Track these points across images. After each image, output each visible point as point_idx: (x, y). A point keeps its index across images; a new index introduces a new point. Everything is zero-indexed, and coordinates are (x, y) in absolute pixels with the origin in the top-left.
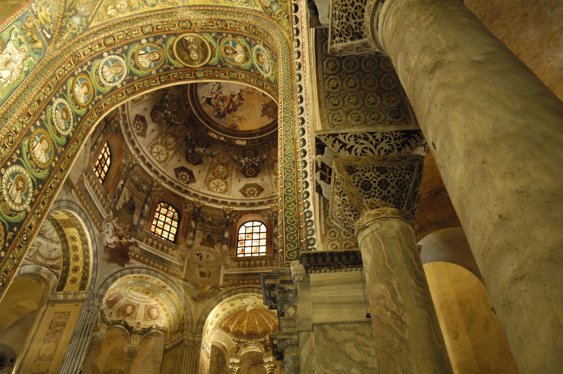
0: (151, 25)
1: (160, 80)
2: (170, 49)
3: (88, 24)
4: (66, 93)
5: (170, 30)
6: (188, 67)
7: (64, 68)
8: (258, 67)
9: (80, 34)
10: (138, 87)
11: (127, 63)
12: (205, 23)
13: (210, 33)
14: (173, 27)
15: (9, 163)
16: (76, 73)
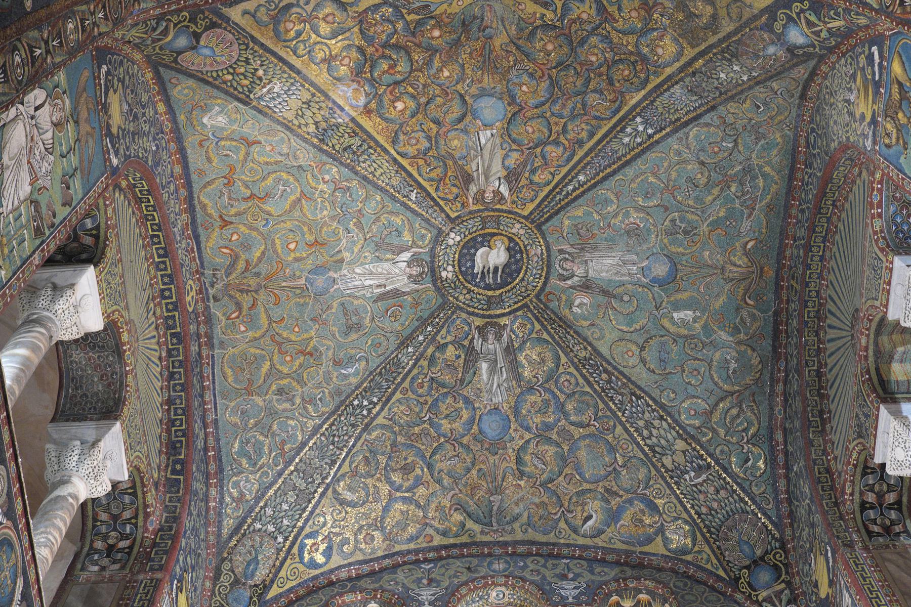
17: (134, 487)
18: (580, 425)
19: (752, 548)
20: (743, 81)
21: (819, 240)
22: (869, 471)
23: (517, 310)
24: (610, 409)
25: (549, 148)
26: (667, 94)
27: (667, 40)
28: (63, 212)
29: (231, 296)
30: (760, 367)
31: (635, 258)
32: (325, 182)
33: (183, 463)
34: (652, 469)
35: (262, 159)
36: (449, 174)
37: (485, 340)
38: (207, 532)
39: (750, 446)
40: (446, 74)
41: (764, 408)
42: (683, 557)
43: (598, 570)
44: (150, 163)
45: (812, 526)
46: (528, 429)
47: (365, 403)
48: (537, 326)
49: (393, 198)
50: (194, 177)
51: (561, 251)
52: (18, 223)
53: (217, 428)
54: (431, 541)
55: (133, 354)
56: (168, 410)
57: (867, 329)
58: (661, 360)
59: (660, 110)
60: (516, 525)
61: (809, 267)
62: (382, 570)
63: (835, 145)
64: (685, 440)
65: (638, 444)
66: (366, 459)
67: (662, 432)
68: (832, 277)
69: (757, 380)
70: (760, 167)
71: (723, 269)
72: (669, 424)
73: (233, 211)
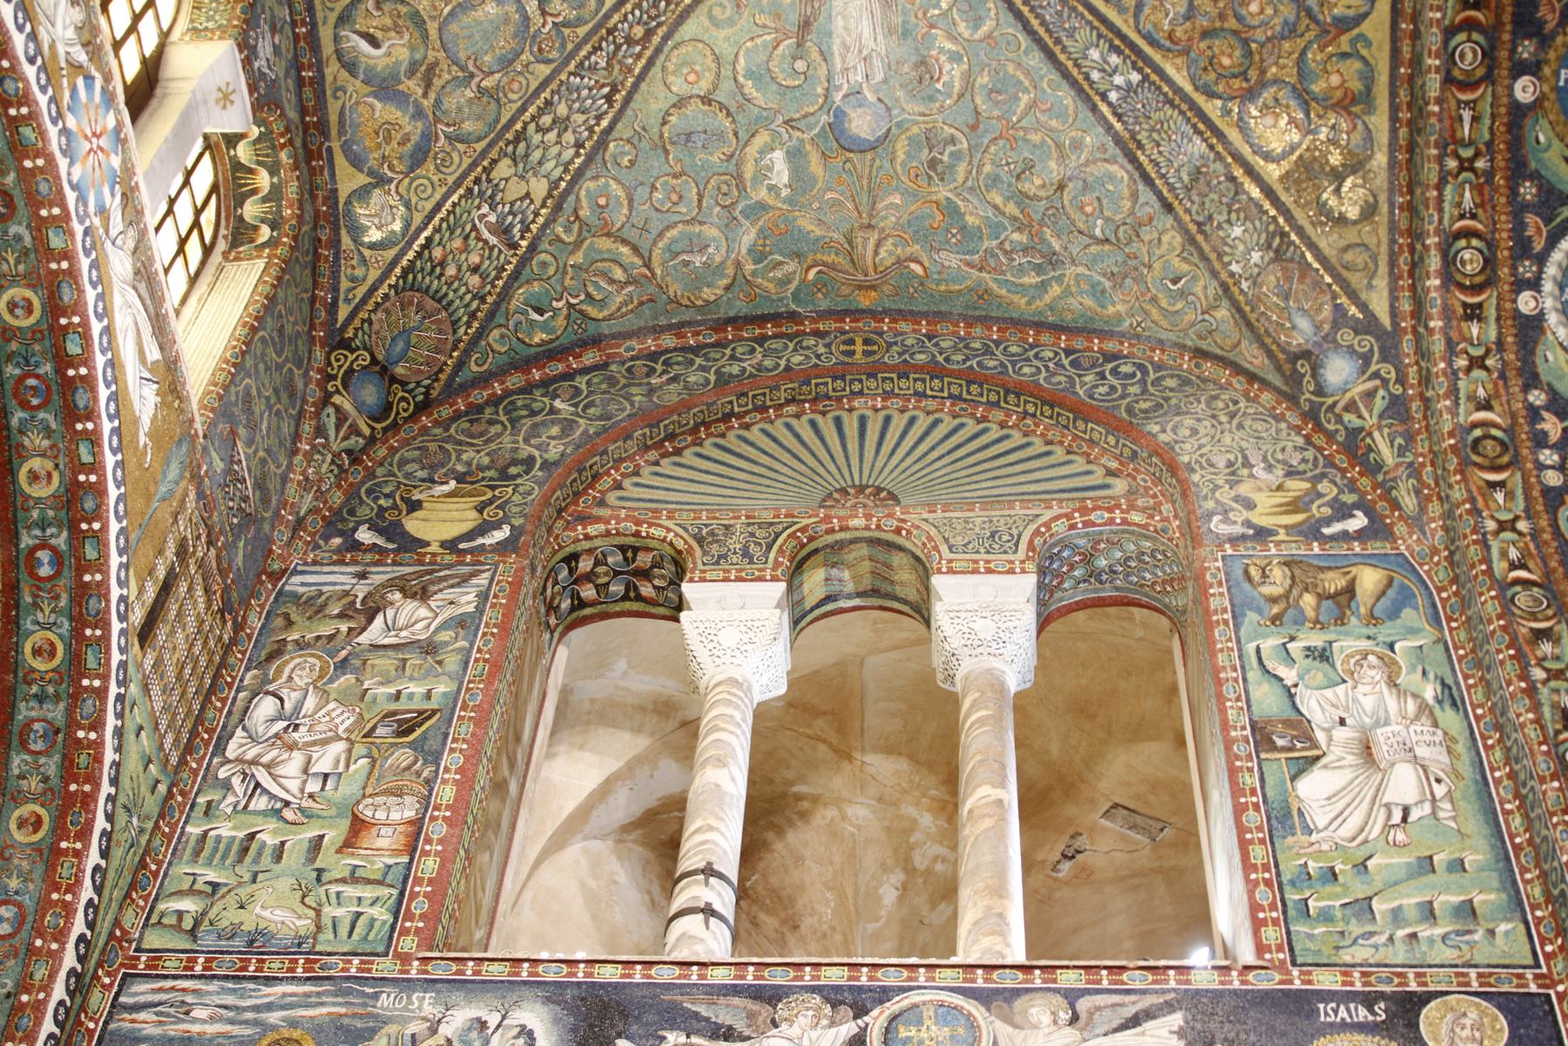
0: (1449, 32)
3: (1369, 325)
7: (1503, 526)
9: (1401, 380)
19: (403, 356)
20: (1230, 263)
21: (955, 390)
22: (630, 554)
24: (578, 47)
26: (1189, 130)
27: (1295, 136)
30: (699, 303)
31: (879, 77)
34: (483, 144)
39: (565, 311)
41: (632, 322)
42: (343, 232)
57: (878, 526)
58: (689, 135)
59: (1156, 116)
61: (903, 375)
64: (550, 195)
65: (523, 109)
67: (554, 150)
69: (678, 303)
70: (1059, 280)
71: (870, 226)
72: (571, 161)
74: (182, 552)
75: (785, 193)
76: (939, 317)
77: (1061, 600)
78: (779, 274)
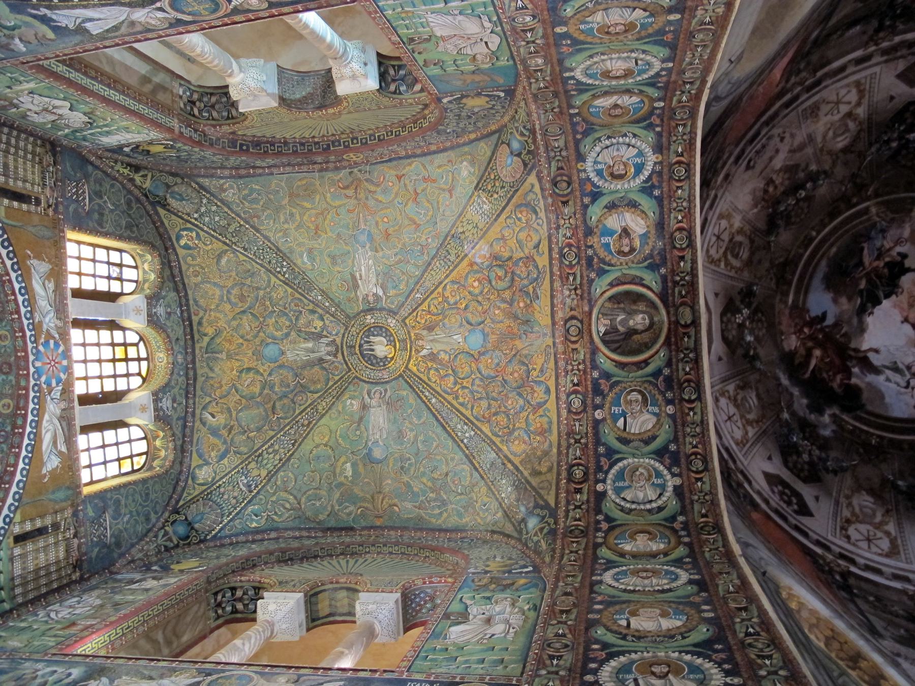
0: (568, 395)
1: (690, 401)
2: (623, 369)
3: (547, 506)
4: (615, 562)
5: (584, 361)
6: (668, 338)
7: (571, 552)
8: (642, 178)
9: (556, 523)
10: (696, 447)
11: (634, 456)
12: (570, 290)
13: (591, 282)
14: (578, 352)
15: (593, 665)
16: (600, 540)
17: (233, 118)
18: (274, 407)
21: (403, 550)
23: (347, 364)
24: (285, 426)
25: (452, 378)
26: (489, 449)
27: (523, 446)
28: (420, 59)
29: (352, 182)
31: (385, 436)
32: (427, 239)
33: (248, 150)
35: (441, 199)
36: (433, 317)
37: (327, 345)
38: (201, 168)
40: (497, 312)
41: (291, 524)
43: (180, 423)
44: (440, 127)
45: (218, 558)
46: (270, 374)
47: (285, 270)
48: (337, 378)
49: (417, 283)
50: (429, 158)
51: (386, 391)
52: (419, 25)
53: (268, 174)
54: (195, 315)
55: (320, 116)
56: (280, 142)
58: (318, 458)
59: (479, 446)
60: (206, 370)
61: (385, 545)
62: (175, 282)
63: (466, 552)
65: (262, 446)
66: (249, 271)
68: (379, 560)
70: (446, 511)
71: (380, 492)
73: (407, 182)
74: (56, 526)
75: (350, 479)
76: (404, 528)
77: (422, 618)
78: (347, 511)
